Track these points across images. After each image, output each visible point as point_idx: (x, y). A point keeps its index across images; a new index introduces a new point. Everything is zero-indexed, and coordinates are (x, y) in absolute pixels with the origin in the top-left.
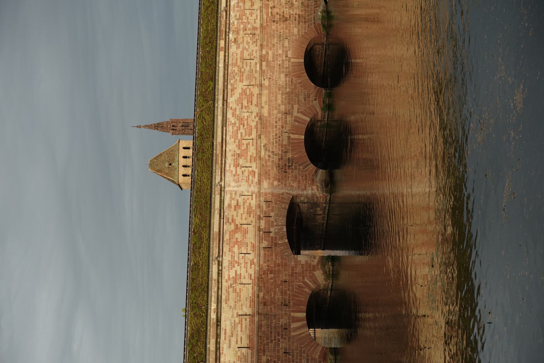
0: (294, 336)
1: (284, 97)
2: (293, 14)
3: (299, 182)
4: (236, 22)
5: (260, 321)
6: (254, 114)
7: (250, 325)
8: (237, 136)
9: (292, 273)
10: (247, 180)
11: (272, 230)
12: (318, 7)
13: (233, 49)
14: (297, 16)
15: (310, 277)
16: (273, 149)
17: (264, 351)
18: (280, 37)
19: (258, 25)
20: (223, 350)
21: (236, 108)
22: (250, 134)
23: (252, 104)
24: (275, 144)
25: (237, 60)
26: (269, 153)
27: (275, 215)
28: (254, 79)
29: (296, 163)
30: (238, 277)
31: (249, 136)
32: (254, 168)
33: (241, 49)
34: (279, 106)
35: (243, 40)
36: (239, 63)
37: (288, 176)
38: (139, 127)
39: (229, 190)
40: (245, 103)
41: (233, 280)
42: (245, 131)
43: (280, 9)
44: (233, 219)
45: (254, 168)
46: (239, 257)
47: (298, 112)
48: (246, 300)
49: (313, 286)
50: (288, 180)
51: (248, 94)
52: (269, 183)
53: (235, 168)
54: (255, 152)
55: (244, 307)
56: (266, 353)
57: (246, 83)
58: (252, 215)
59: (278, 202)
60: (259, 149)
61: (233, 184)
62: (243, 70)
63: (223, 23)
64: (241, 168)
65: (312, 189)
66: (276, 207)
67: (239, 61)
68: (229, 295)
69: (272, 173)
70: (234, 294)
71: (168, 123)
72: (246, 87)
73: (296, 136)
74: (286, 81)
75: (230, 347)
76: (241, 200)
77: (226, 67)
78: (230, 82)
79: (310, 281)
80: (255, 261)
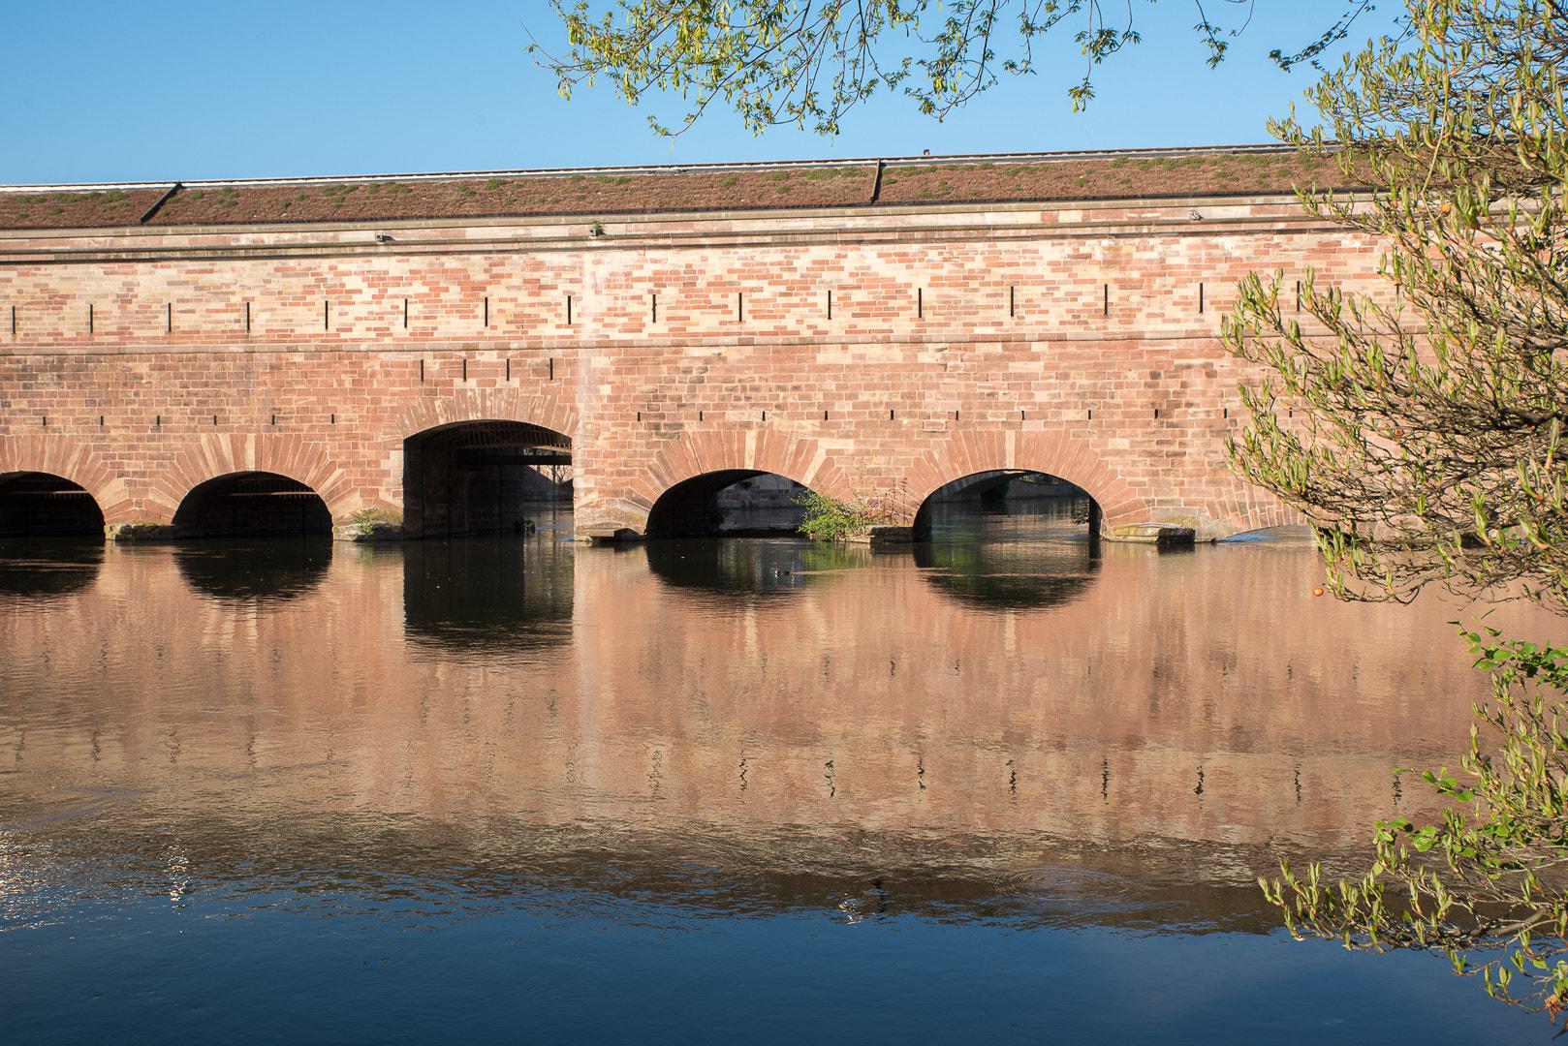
0: (198, 440)
1: (882, 409)
2: (1183, 434)
3: (608, 455)
4: (1147, 255)
5: (234, 356)
6: (823, 324)
7: (223, 332)
8: (747, 278)
10: (616, 309)
11: (472, 382)
12: (1215, 515)
13: (1050, 252)
14: (1176, 448)
15: (346, 483)
16: (710, 380)
17: (161, 368)
18: (1095, 394)
19: (1143, 325)
20: (162, 267)
21: (842, 269)
22: (756, 315)
23: (854, 315)
24: (724, 385)
25: (1010, 265)
26: (700, 368)
27: (514, 390)
28: (941, 319)
29: (666, 445)
30: (344, 297)
31: (750, 312)
32: (650, 328)
33: (1049, 276)
35: (1084, 282)
36: (997, 273)
37: (626, 425)
39: (583, 262)
40: (858, 296)
41: (335, 285)
42: (766, 301)
43: (1204, 393)
44: (502, 276)
45: (650, 328)
46: (396, 297)
47: (828, 452)
48: (286, 321)
49: (321, 491)
50: (614, 425)
51: (891, 303)
52: (605, 372)
53: (651, 275)
54: (701, 329)
55: (267, 315)
56: (156, 374)
58: (512, 327)
59: (549, 397)
60: (705, 340)
61: (602, 272)
62: (974, 284)
63: (1149, 215)
64: (650, 291)
65: (589, 491)
66: (536, 392)
68: (298, 275)
69: (635, 379)
70: (300, 290)
72: (916, 298)
73: (751, 444)
74: (936, 415)
75: (170, 283)
76: (557, 296)
77: (983, 233)
78: (931, 248)
79: (335, 483)
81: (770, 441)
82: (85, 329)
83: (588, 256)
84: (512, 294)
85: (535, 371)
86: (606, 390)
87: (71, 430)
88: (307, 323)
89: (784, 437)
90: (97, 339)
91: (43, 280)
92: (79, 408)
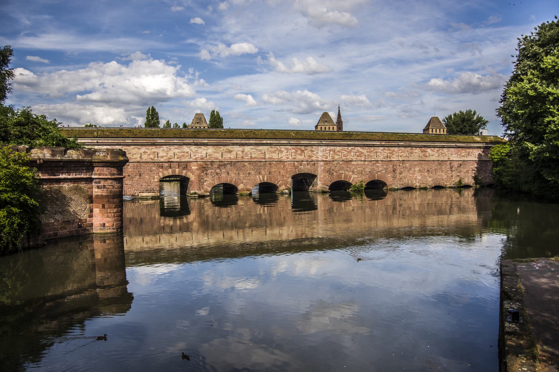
3: (323, 178)
6: (352, 158)
9: (283, 176)
11: (302, 167)
17: (250, 164)
22: (344, 156)
30: (281, 152)
33: (381, 152)
34: (356, 169)
38: (339, 108)
40: (357, 154)
45: (329, 158)
47: (354, 177)
52: (322, 165)
54: (336, 158)
55: (268, 155)
56: (249, 165)
57: (366, 154)
58: (308, 158)
61: (322, 149)
62: (372, 152)
65: (320, 184)
67: (376, 151)
71: (341, 120)
76: (315, 152)
77: (374, 146)
80: (289, 160)
81: (346, 176)
82: (236, 157)
83: (320, 147)
84: (308, 152)
85: (312, 165)
86: (323, 168)
87: (233, 175)
88: (275, 156)
89: (347, 175)
91: (228, 148)
92: (235, 171)
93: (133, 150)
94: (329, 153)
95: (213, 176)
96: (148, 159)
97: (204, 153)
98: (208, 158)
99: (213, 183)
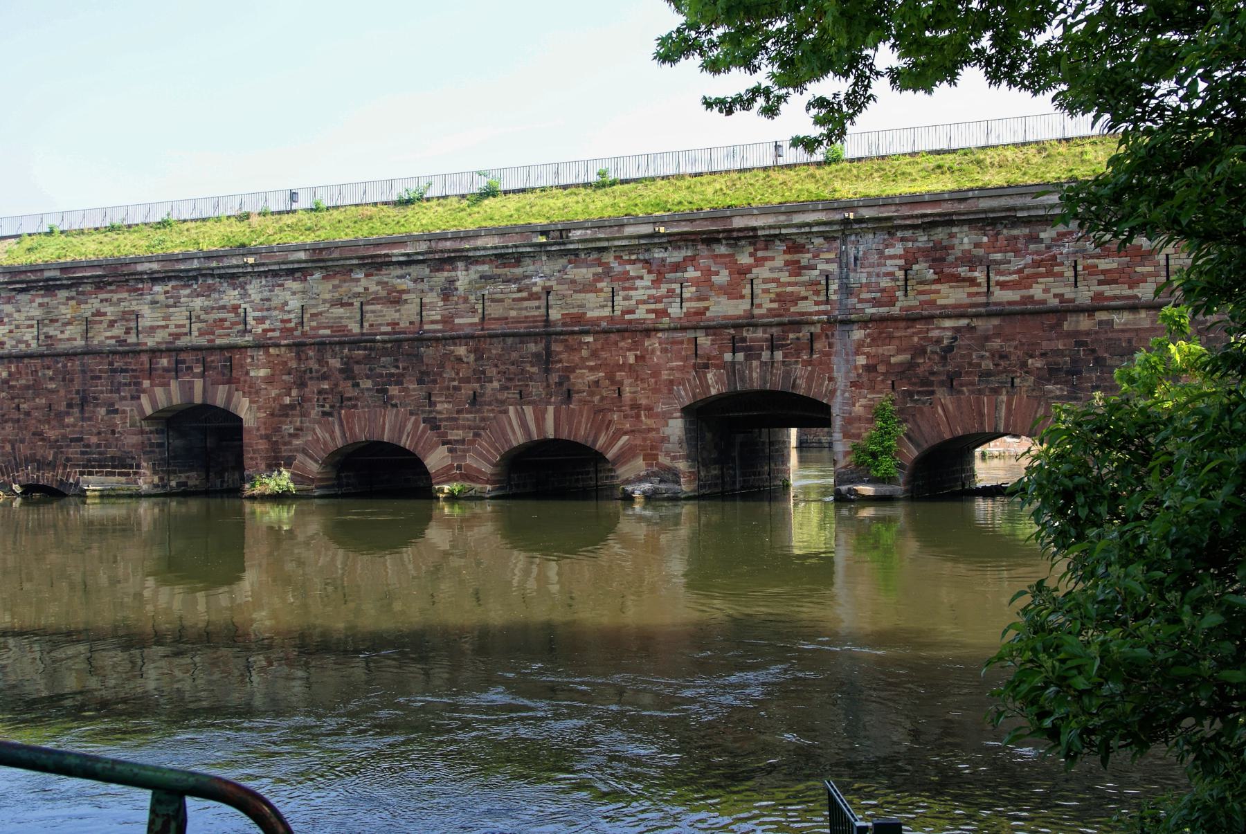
0: (506, 412)
6: (1068, 293)
23: (1100, 283)
44: (766, 259)
58: (775, 305)
64: (900, 268)
82: (417, 319)
86: (862, 360)
88: (595, 308)
90: (426, 327)
93: (63, 310)
94: (900, 274)
95: (327, 408)
96: (108, 342)
97: (294, 304)
98: (307, 328)
99: (325, 443)
